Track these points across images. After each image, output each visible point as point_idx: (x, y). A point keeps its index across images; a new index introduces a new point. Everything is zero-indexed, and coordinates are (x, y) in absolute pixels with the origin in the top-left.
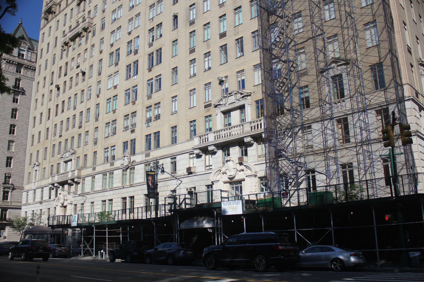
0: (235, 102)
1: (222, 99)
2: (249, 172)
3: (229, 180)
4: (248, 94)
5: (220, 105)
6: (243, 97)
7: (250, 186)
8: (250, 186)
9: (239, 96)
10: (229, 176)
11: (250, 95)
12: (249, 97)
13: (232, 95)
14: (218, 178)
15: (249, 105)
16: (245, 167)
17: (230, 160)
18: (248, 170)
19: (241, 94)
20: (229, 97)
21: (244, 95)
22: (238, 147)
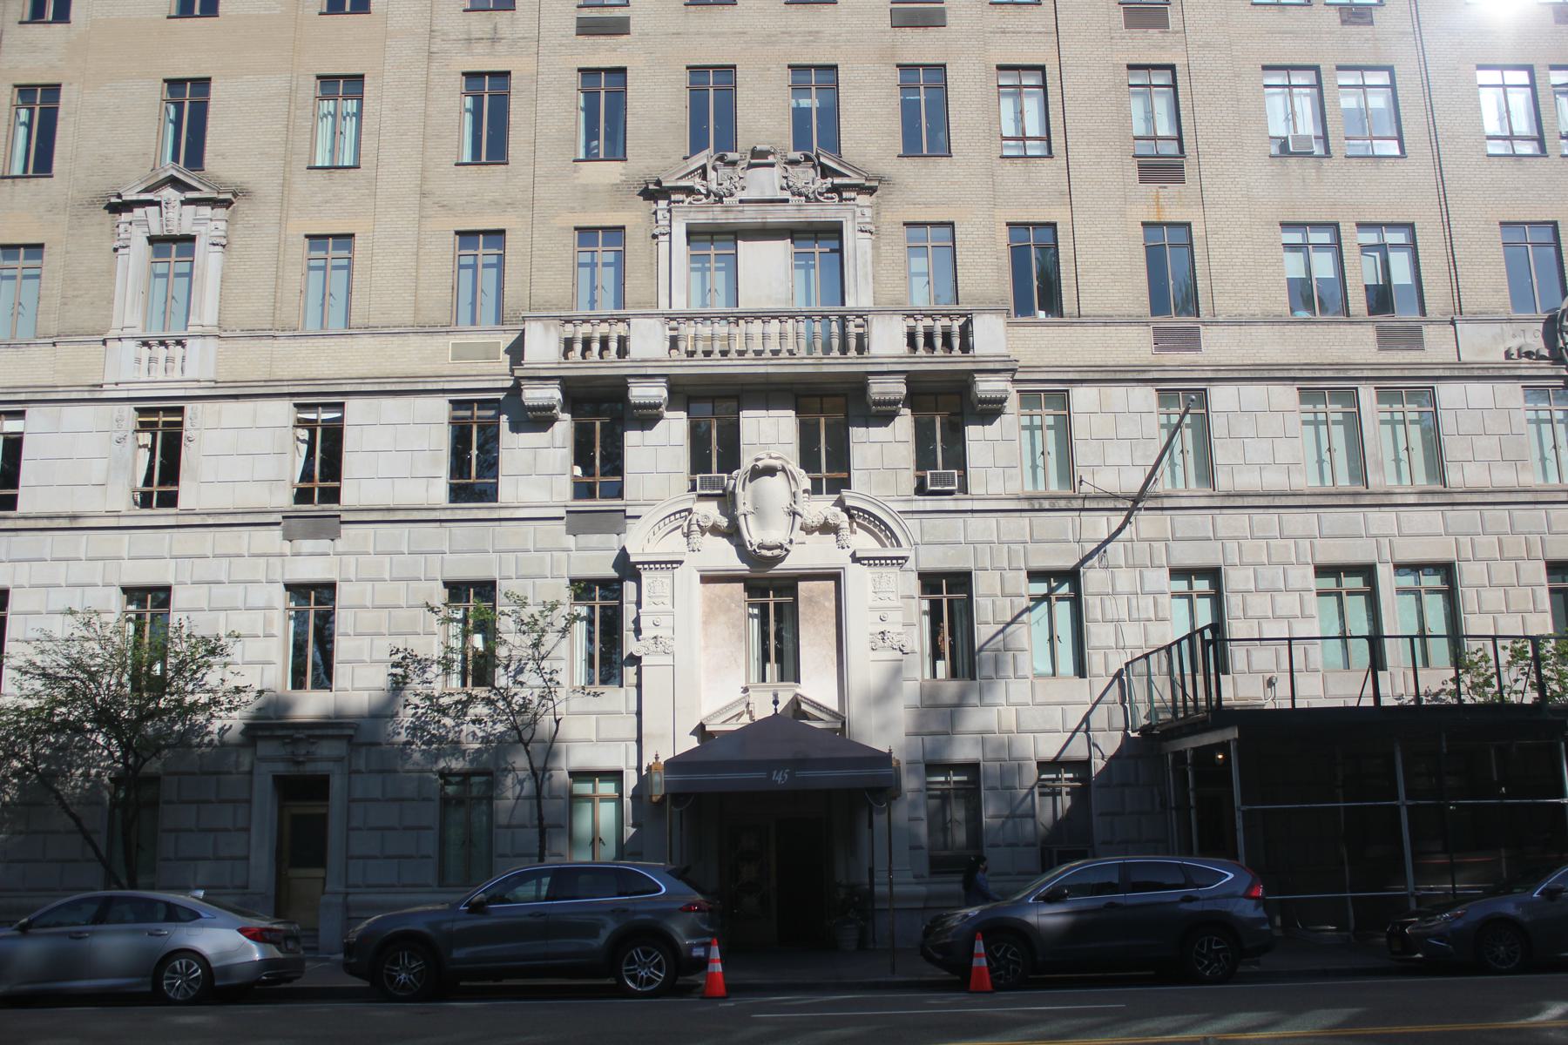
0: (787, 201)
1: (704, 168)
2: (864, 542)
3: (745, 566)
4: (867, 184)
5: (690, 191)
6: (836, 189)
7: (872, 609)
8: (872, 609)
9: (806, 177)
10: (762, 546)
11: (871, 191)
12: (863, 199)
13: (772, 165)
14: (673, 545)
15: (868, 235)
16: (845, 517)
17: (784, 470)
18: (859, 530)
19: (826, 172)
20: (751, 166)
21: (846, 181)
22: (792, 413)
